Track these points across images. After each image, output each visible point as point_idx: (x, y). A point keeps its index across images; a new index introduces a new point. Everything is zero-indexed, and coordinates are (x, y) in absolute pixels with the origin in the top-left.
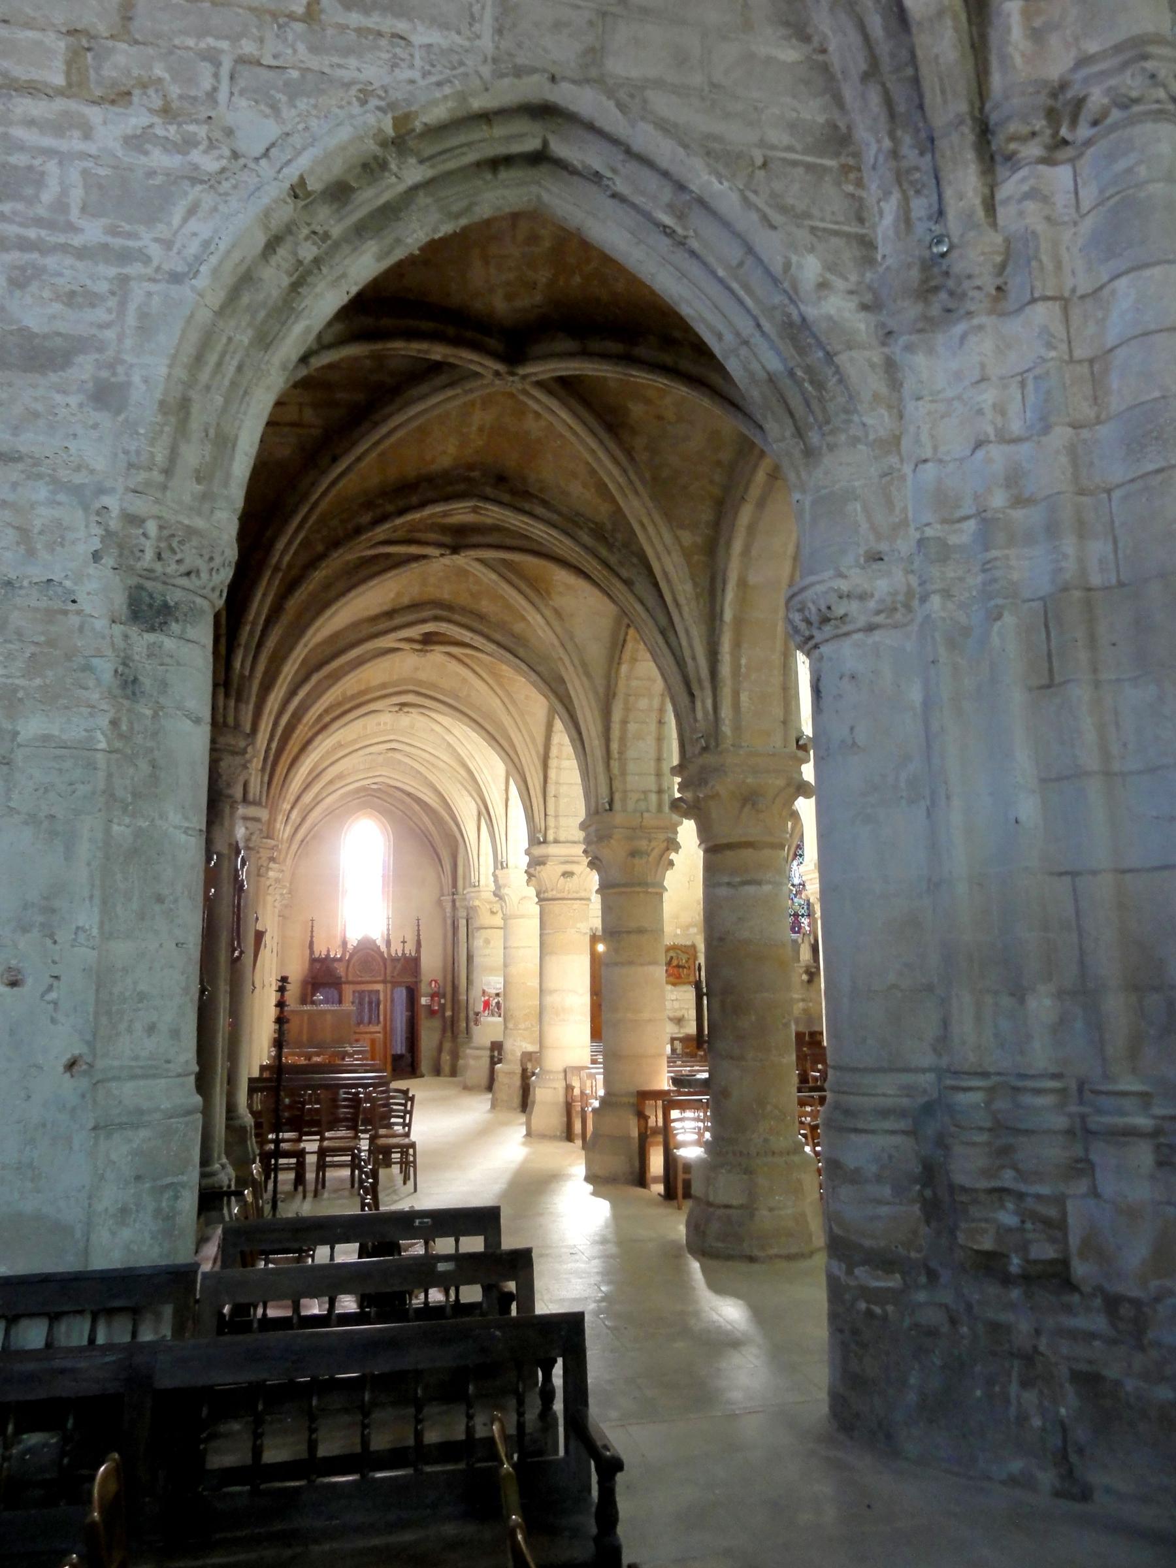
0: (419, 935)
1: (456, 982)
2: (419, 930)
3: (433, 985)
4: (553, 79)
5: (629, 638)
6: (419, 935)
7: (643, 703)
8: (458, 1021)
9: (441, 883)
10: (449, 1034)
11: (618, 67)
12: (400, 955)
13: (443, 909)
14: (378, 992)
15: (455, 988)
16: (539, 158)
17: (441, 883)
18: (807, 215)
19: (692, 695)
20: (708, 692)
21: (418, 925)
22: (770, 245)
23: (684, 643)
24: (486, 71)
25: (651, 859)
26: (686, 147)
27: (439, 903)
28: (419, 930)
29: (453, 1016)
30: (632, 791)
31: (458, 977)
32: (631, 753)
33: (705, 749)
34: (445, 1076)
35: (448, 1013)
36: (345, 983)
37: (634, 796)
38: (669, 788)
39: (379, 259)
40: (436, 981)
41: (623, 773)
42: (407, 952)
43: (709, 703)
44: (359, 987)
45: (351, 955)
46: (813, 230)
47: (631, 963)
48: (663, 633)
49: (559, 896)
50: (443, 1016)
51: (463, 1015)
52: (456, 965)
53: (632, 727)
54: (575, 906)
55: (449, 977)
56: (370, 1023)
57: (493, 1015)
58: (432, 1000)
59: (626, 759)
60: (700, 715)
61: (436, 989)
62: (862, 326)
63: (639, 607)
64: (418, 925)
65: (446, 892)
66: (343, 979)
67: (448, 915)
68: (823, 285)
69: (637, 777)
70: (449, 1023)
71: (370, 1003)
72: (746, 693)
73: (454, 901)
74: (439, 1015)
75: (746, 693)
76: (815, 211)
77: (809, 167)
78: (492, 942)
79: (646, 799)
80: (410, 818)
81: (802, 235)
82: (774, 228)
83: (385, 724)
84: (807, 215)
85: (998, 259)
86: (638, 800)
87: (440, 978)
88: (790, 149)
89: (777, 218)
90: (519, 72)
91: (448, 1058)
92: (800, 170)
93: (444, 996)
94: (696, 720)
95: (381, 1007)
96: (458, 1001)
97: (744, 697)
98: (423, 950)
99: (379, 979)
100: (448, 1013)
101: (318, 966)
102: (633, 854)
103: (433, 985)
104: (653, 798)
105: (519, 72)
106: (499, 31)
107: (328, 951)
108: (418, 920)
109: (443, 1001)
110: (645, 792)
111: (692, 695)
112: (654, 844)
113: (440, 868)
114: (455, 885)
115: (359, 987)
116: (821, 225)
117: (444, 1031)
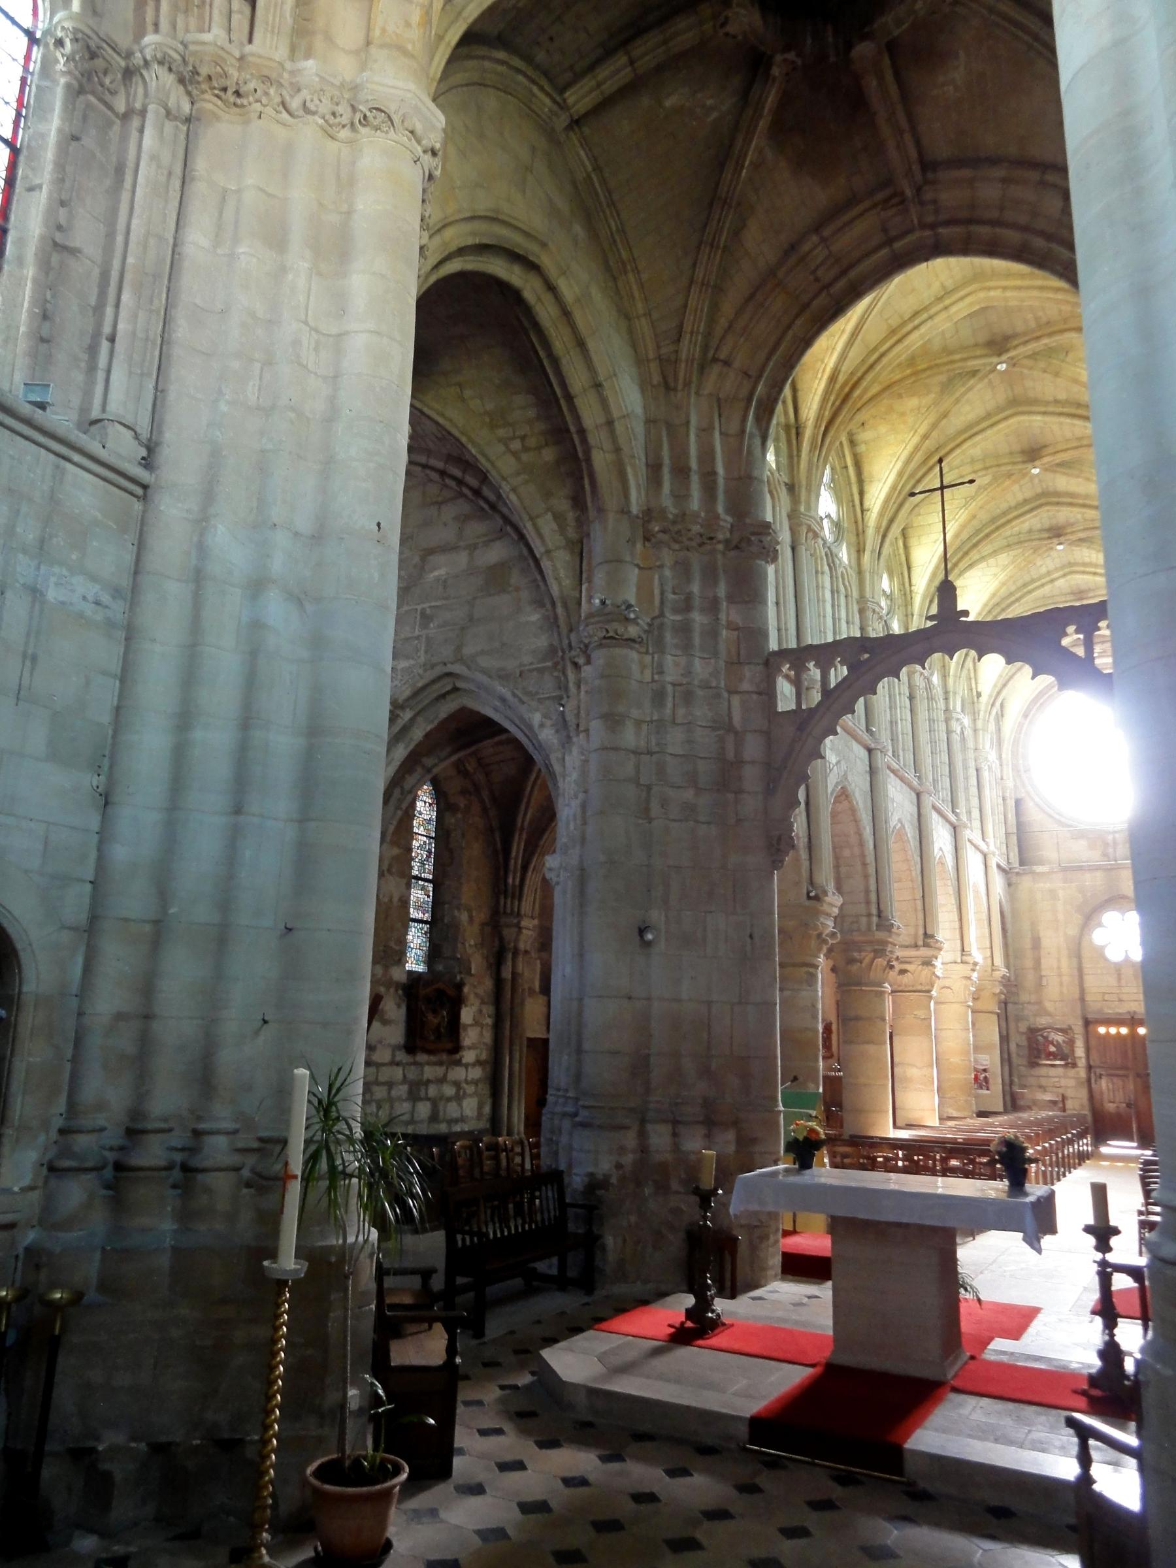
4: (445, 664)
11: (467, 651)
16: (455, 689)
18: (537, 693)
22: (523, 709)
24: (421, 671)
25: (863, 965)
26: (490, 677)
39: (406, 748)
46: (539, 699)
47: (851, 1042)
49: (900, 989)
54: (912, 998)
57: (982, 1088)
62: (555, 741)
68: (542, 725)
76: (541, 691)
77: (538, 670)
81: (534, 704)
82: (523, 703)
84: (537, 693)
85: (576, 712)
86: (852, 923)
88: (531, 664)
89: (525, 699)
90: (433, 666)
92: (535, 673)
102: (852, 961)
105: (433, 666)
106: (426, 652)
110: (857, 916)
112: (863, 954)
116: (542, 696)
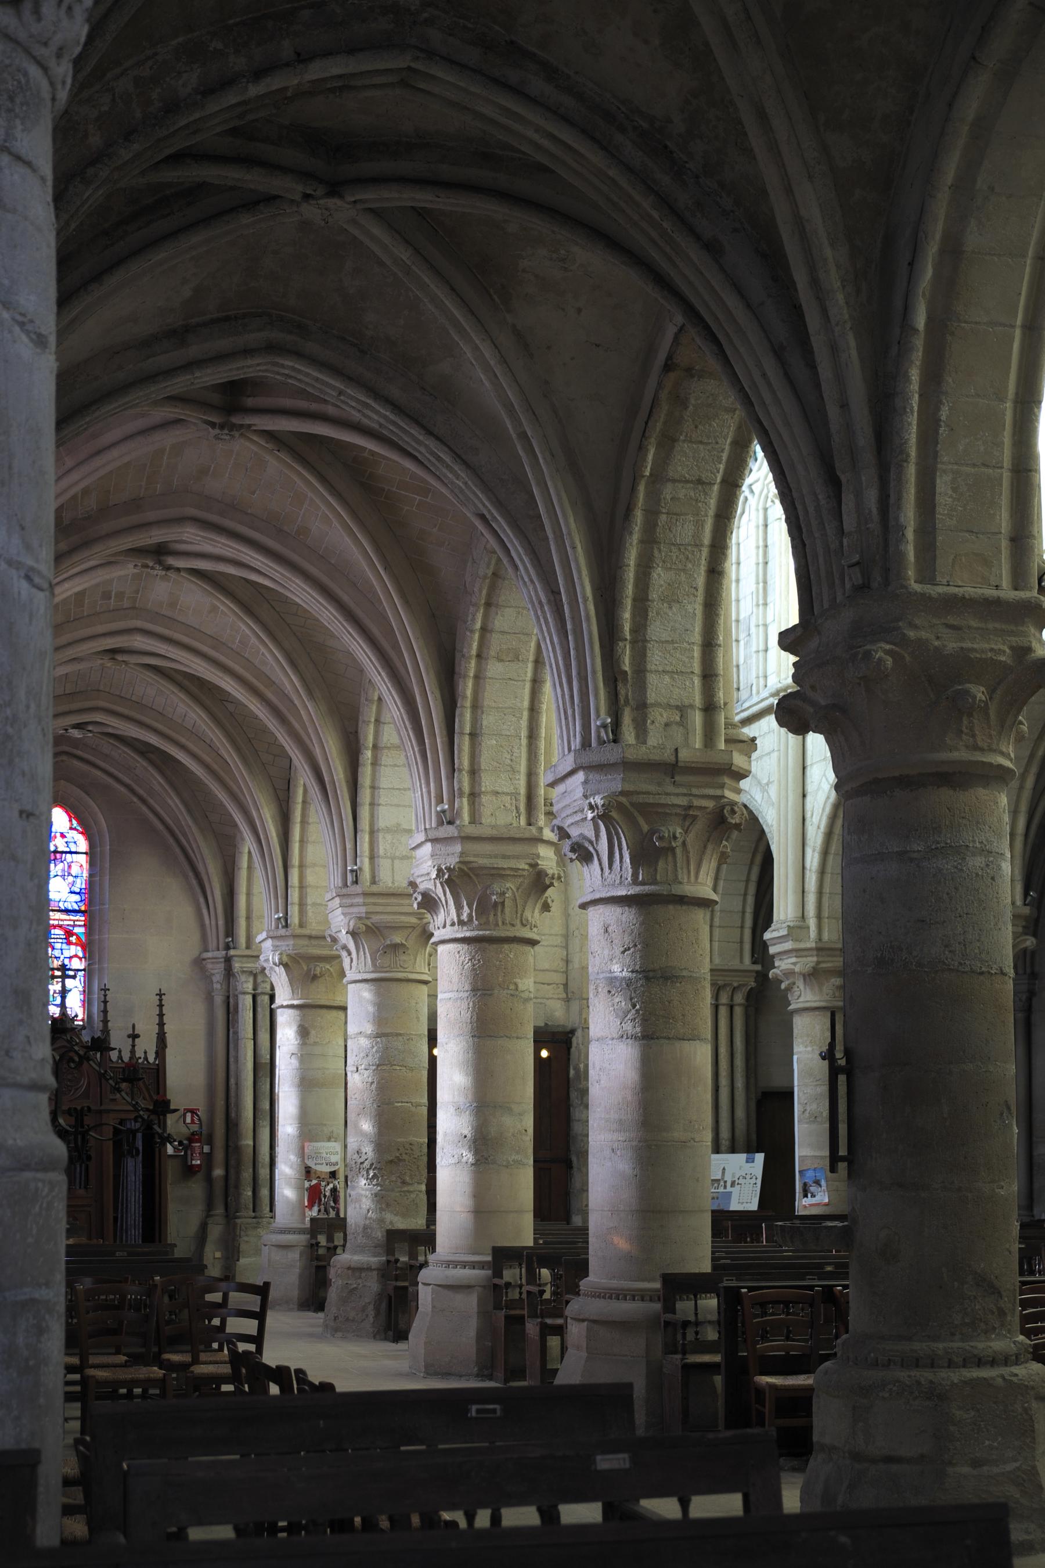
0: (161, 1024)
1: (233, 1115)
3: (188, 1120)
5: (664, 395)
6: (161, 1024)
7: (684, 532)
8: (237, 1186)
9: (202, 926)
12: (126, 1059)
13: (207, 978)
15: (232, 1125)
19: (834, 484)
20: (869, 476)
21: (161, 1006)
23: (825, 371)
27: (199, 963)
29: (226, 1177)
30: (657, 705)
31: (237, 1105)
32: (656, 630)
33: (863, 588)
35: (218, 1172)
37: (658, 717)
38: (725, 704)
41: (641, 669)
42: (139, 1053)
43: (871, 497)
48: (778, 353)
50: (209, 1179)
51: (247, 1175)
52: (232, 1081)
53: (660, 577)
55: (220, 1103)
59: (645, 641)
60: (849, 522)
61: (195, 1128)
63: (732, 301)
64: (161, 1006)
65: (212, 944)
67: (217, 986)
69: (667, 679)
72: (947, 478)
73: (228, 960)
74: (200, 1176)
75: (947, 478)
78: (313, 1032)
79: (683, 722)
83: (120, 595)
87: (199, 1102)
93: (210, 1141)
94: (841, 532)
96: (238, 1149)
97: (943, 484)
98: (169, 1052)
100: (218, 1172)
103: (188, 1120)
104: (697, 719)
108: (160, 995)
110: (682, 710)
111: (834, 484)
114: (230, 929)
117: (210, 1206)
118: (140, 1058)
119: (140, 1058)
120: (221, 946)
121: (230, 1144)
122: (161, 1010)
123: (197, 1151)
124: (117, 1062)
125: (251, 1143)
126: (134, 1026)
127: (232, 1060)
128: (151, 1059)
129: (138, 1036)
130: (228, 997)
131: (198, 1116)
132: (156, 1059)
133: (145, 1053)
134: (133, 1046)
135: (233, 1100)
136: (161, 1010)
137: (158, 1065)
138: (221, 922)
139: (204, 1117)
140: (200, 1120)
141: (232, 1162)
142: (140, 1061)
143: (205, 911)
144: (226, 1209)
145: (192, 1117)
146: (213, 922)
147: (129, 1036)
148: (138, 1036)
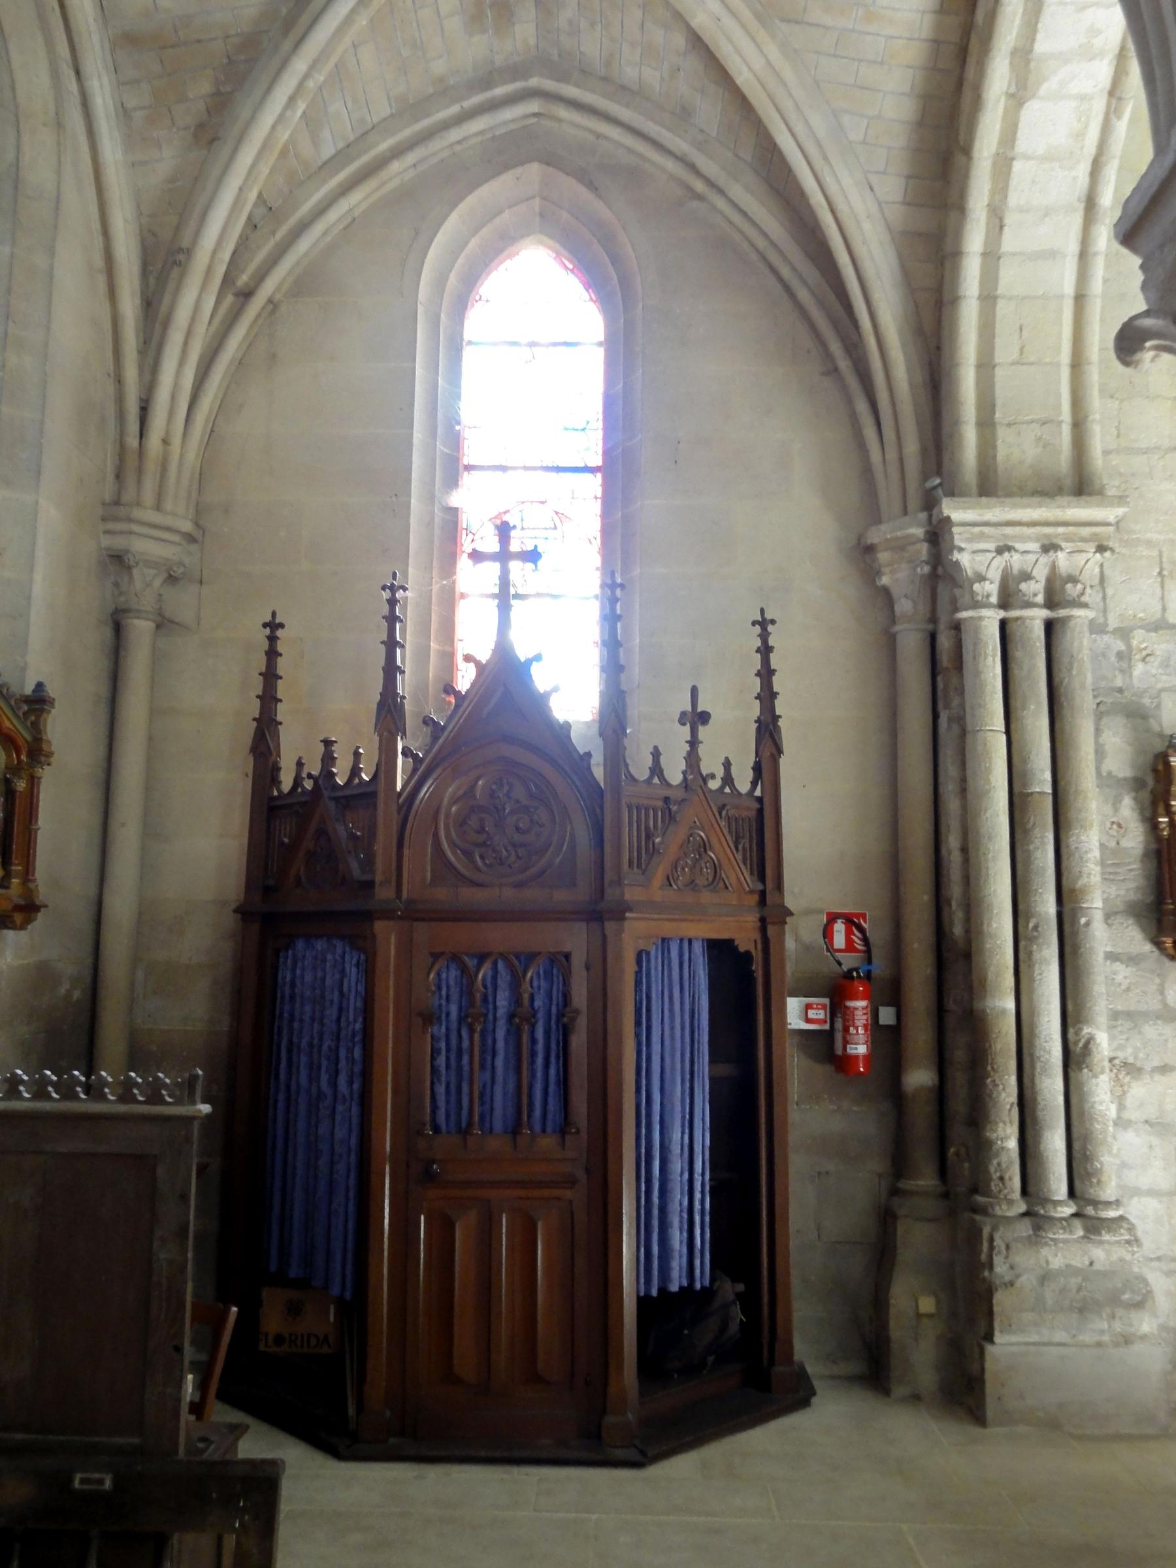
0: (767, 696)
1: (958, 930)
2: (766, 673)
3: (839, 940)
6: (767, 696)
10: (925, 1180)
12: (675, 773)
14: (560, 962)
17: (867, 471)
21: (765, 650)
28: (766, 673)
29: (941, 1092)
34: (915, 1398)
36: (387, 914)
40: (851, 921)
42: (711, 764)
44: (461, 936)
45: (421, 771)
51: (1007, 1093)
52: (952, 842)
55: (919, 898)
56: (515, 1130)
58: (837, 1008)
61: (849, 961)
64: (765, 650)
65: (889, 496)
66: (384, 893)
67: (903, 606)
70: (921, 1119)
71: (519, 1019)
80: (721, 192)
91: (927, 1304)
95: (579, 1041)
99: (562, 897)
101: (285, 833)
103: (839, 940)
107: (328, 759)
108: (764, 624)
109: (887, 1016)
113: (862, 406)
115: (461, 936)
118: (713, 776)
119: (713, 776)
120: (914, 501)
121: (951, 1005)
122: (766, 661)
123: (861, 1019)
124: (649, 781)
125: (1010, 1005)
126: (694, 692)
127: (949, 788)
128: (743, 786)
129: (704, 717)
130: (933, 637)
131: (861, 930)
132: (754, 784)
133: (727, 764)
134: (694, 743)
135: (955, 891)
136: (766, 661)
137: (760, 800)
138: (912, 447)
139: (879, 935)
140: (865, 940)
141: (959, 1055)
142: (714, 785)
143: (870, 432)
144: (943, 1172)
145: (849, 933)
146: (892, 455)
147: (682, 721)
148: (704, 717)
